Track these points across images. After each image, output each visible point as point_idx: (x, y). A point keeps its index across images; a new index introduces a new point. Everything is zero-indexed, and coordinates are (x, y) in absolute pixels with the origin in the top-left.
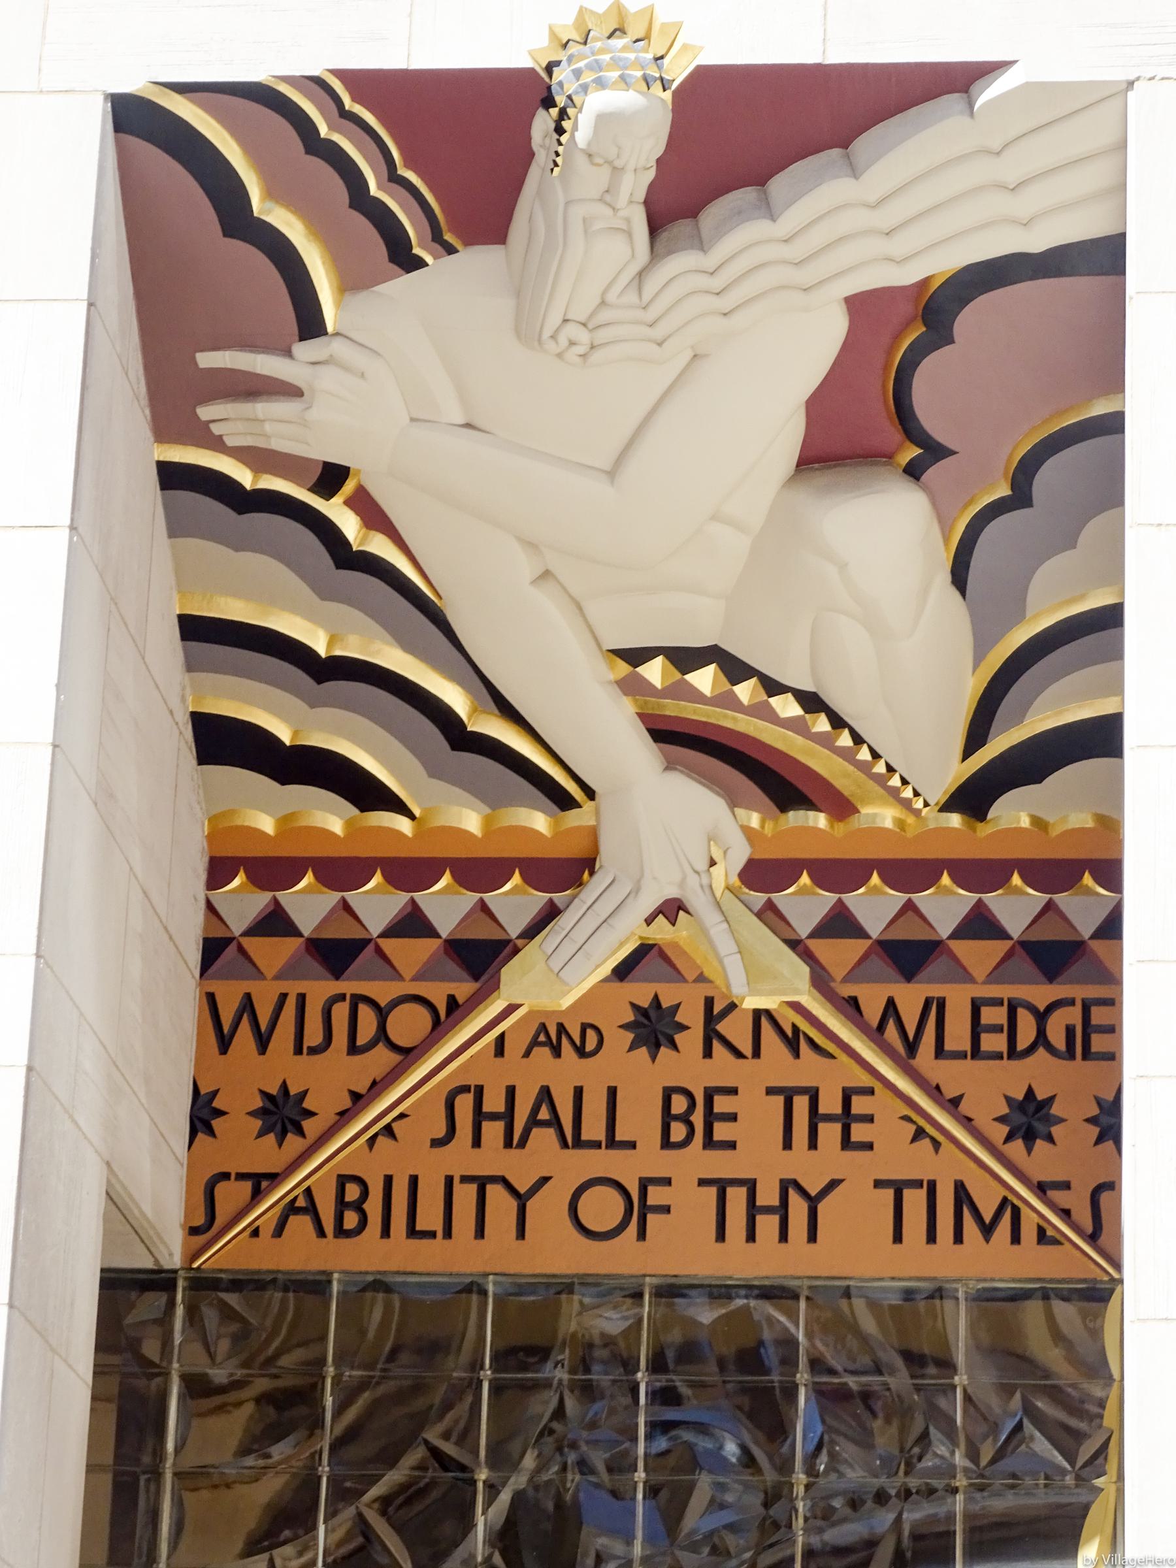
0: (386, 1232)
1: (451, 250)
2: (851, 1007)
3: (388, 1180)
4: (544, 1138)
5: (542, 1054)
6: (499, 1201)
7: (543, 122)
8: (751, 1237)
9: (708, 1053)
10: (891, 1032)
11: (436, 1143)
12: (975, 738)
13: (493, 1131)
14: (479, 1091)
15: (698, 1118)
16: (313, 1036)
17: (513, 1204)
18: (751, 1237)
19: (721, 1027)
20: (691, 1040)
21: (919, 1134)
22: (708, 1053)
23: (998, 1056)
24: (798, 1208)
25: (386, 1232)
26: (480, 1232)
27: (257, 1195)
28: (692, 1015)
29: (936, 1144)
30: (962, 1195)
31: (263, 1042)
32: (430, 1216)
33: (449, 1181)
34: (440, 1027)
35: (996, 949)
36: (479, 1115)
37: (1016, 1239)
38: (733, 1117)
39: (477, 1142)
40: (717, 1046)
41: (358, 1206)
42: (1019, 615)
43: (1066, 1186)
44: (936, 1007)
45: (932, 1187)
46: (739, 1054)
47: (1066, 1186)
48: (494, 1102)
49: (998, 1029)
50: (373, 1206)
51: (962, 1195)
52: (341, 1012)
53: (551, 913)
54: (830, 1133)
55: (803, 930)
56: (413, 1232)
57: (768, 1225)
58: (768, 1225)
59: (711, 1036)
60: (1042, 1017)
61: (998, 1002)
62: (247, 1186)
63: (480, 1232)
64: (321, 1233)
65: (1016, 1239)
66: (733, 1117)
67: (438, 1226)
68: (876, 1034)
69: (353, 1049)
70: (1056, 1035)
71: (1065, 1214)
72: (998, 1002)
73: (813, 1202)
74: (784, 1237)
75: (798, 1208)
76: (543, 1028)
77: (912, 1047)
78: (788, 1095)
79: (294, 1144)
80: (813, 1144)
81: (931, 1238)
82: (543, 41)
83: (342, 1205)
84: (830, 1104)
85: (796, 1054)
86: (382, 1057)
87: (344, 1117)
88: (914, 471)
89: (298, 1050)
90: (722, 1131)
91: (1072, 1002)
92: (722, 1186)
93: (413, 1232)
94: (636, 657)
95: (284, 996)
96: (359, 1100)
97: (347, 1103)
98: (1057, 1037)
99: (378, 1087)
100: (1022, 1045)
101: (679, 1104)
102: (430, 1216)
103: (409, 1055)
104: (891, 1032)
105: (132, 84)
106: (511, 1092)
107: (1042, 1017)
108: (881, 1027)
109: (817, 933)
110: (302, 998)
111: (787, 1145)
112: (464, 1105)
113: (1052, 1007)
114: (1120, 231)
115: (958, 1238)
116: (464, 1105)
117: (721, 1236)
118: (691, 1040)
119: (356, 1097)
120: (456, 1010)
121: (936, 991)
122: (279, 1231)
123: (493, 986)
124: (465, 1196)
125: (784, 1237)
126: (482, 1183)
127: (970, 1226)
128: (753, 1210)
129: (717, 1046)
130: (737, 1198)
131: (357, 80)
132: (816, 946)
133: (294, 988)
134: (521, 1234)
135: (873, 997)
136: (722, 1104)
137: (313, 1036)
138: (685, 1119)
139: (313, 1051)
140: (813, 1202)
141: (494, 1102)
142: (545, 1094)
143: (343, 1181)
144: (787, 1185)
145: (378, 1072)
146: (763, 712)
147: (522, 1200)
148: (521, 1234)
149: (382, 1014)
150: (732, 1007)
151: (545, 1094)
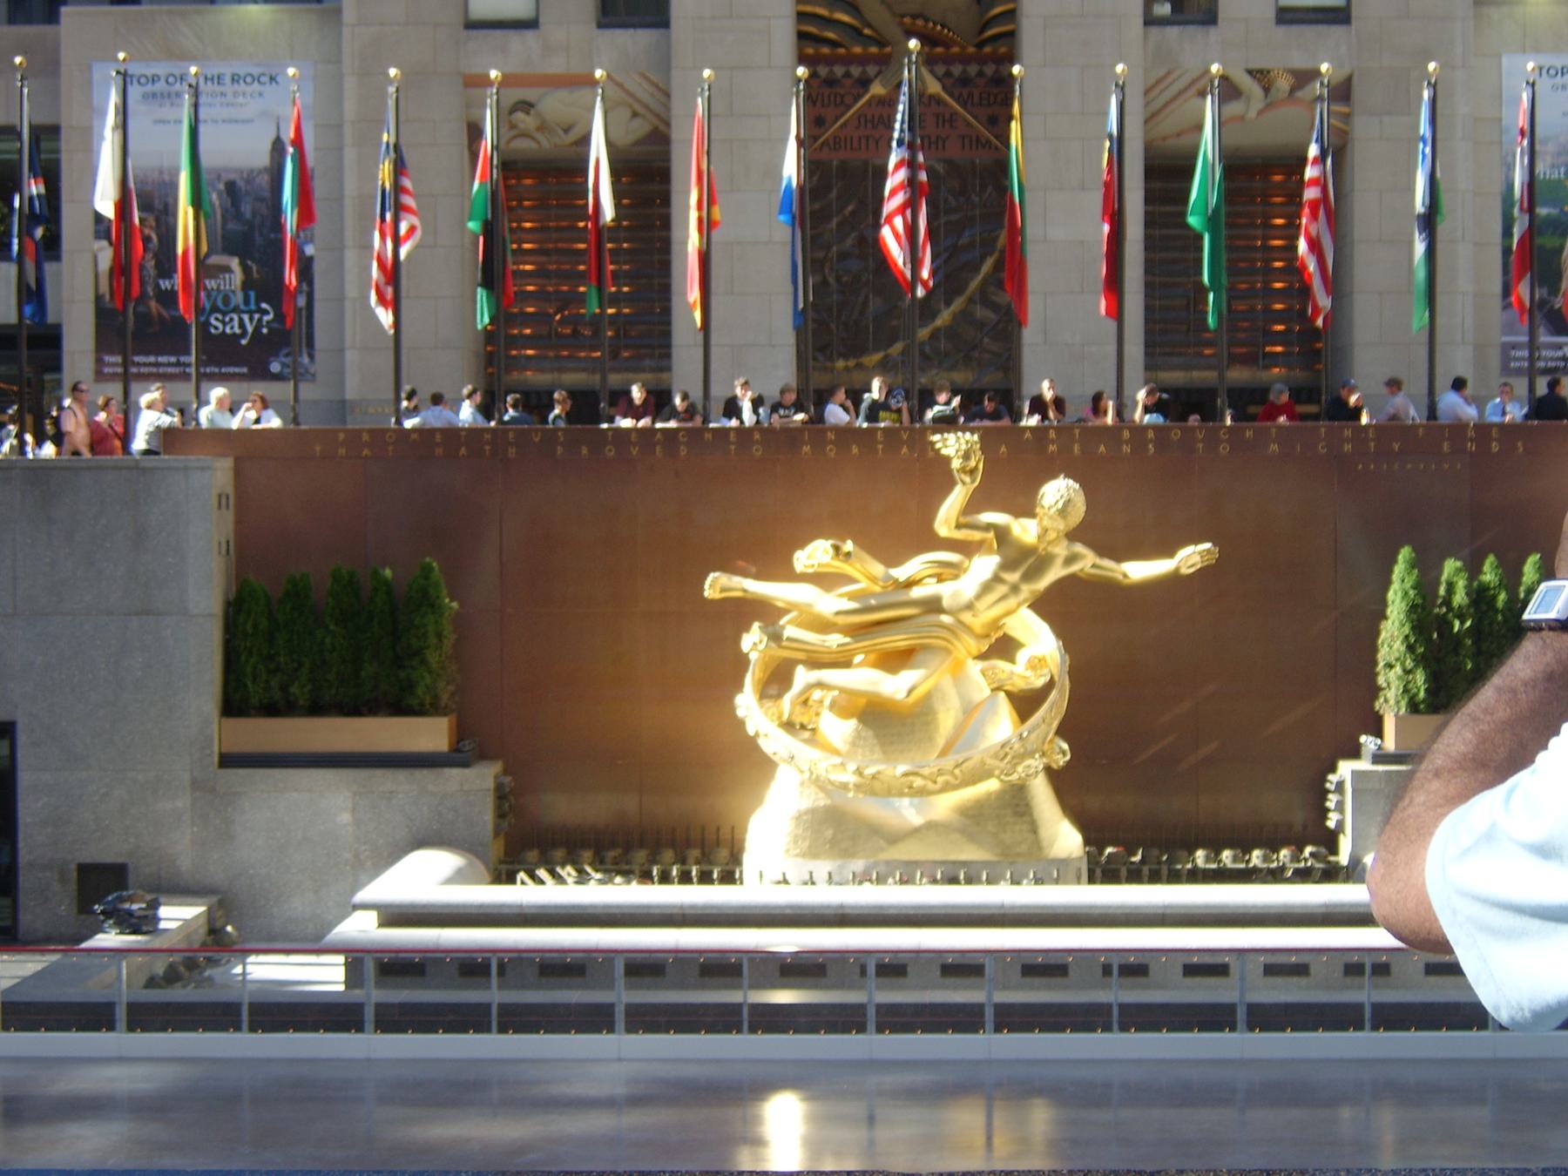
2: (951, 95)
10: (961, 100)
13: (869, 125)
16: (826, 101)
32: (855, 145)
36: (866, 121)
42: (992, 6)
44: (971, 95)
48: (869, 117)
50: (843, 144)
54: (947, 125)
57: (933, 146)
58: (933, 146)
64: (830, 149)
68: (958, 101)
70: (999, 99)
74: (937, 148)
93: (852, 149)
102: (855, 145)
103: (849, 107)
120: (857, 98)
123: (866, 90)
124: (863, 141)
135: (956, 93)
141: (869, 117)
149: (842, 97)
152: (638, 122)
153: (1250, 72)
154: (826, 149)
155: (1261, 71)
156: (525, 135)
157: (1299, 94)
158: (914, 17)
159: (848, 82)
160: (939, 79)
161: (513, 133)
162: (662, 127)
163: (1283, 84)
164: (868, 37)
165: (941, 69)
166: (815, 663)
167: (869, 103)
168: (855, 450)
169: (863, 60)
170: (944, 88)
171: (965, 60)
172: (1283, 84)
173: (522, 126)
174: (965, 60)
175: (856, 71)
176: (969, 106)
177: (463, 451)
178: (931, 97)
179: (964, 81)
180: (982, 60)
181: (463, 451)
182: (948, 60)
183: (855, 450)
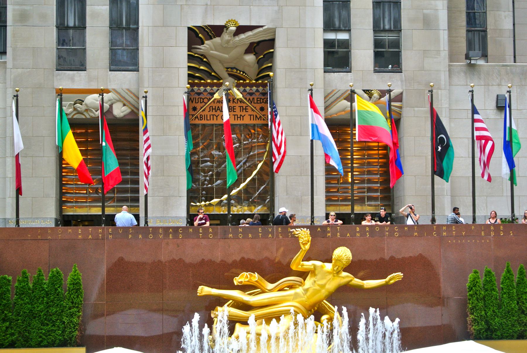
0: (205, 120)
1: (215, 38)
2: (246, 99)
3: (205, 115)
4: (218, 111)
5: (218, 103)
6: (215, 117)
7: (225, 29)
8: (237, 120)
9: (233, 103)
10: (250, 101)
11: (209, 112)
12: (258, 75)
13: (214, 110)
14: (212, 107)
15: (232, 109)
16: (197, 101)
17: (216, 117)
18: (237, 120)
19: (234, 101)
20: (231, 102)
21: (252, 110)
22: (233, 103)
23: (259, 103)
24: (242, 117)
25: (205, 120)
26: (213, 120)
27: (193, 116)
28: (231, 99)
29: (254, 111)
30: (256, 116)
31: (192, 102)
32: (209, 118)
33: (210, 115)
34: (208, 101)
35: (259, 93)
36: (213, 109)
37: (261, 120)
38: (235, 109)
39: (212, 111)
40: (234, 103)
41: (202, 117)
43: (265, 115)
44: (253, 99)
45: (253, 115)
46: (236, 103)
47: (265, 115)
48: (214, 108)
49: (259, 101)
50: (203, 117)
51: (256, 116)
52: (199, 99)
53: (218, 90)
54: (244, 110)
55: (241, 91)
56: (207, 120)
57: (239, 119)
58: (239, 119)
59: (233, 101)
60: (263, 100)
61: (259, 98)
62: (192, 116)
63: (213, 120)
64: (199, 120)
65: (261, 120)
66: (235, 109)
67: (209, 119)
68: (248, 101)
69: (201, 103)
71: (265, 118)
72: (259, 98)
73: (243, 117)
74: (240, 120)
75: (242, 117)
76: (218, 101)
77: (251, 102)
78: (240, 107)
79: (196, 112)
80: (243, 111)
81: (253, 120)
82: (226, 23)
83: (200, 117)
84: (244, 108)
85: (241, 103)
86: (203, 104)
87: (200, 109)
88: (254, 55)
89: (196, 103)
90: (235, 110)
91: (265, 98)
92: (235, 115)
93: (207, 120)
94: (227, 68)
95: (194, 98)
96: (202, 108)
97: (200, 108)
98: (264, 102)
99: (203, 106)
100: (261, 102)
101: (231, 108)
102: (209, 118)
103: (206, 103)
104: (250, 101)
105: (190, 26)
106: (215, 107)
107: (263, 100)
108: (249, 101)
109: (243, 91)
110: (196, 98)
111: (240, 111)
112: (211, 108)
113: (264, 99)
114: (274, 38)
115: (256, 120)
116: (211, 108)
117: (235, 120)
118: (231, 102)
119: (201, 107)
120: (210, 99)
121: (254, 97)
122: (195, 120)
123: (213, 97)
124: (212, 116)
125: (240, 120)
126: (213, 115)
127: (257, 119)
128: (238, 117)
129: (234, 103)
130: (236, 116)
131: (209, 26)
132: (242, 93)
133: (195, 97)
134: (217, 120)
136: (234, 108)
137: (197, 101)
138: (231, 109)
139: (197, 103)
140: (243, 117)
141: (214, 108)
142: (218, 107)
143: (200, 115)
144: (241, 115)
145: (203, 105)
146: (239, 73)
147: (217, 117)
148: (217, 120)
149: (203, 99)
150: (235, 99)
151: (218, 107)
152: (124, 108)
153: (364, 91)
154: (197, 119)
155: (368, 90)
156: (79, 113)
157: (382, 99)
158: (232, 68)
159: (205, 93)
160: (241, 93)
161: (75, 112)
162: (135, 110)
164: (213, 75)
165: (242, 88)
167: (214, 101)
168: (250, 236)
169: (212, 85)
170: (243, 96)
171: (251, 85)
172: (376, 95)
173: (79, 109)
174: (251, 85)
175: (208, 88)
176: (253, 103)
177: (90, 237)
178: (238, 99)
179: (251, 94)
180: (257, 86)
181: (90, 237)
182: (245, 85)
183: (250, 236)
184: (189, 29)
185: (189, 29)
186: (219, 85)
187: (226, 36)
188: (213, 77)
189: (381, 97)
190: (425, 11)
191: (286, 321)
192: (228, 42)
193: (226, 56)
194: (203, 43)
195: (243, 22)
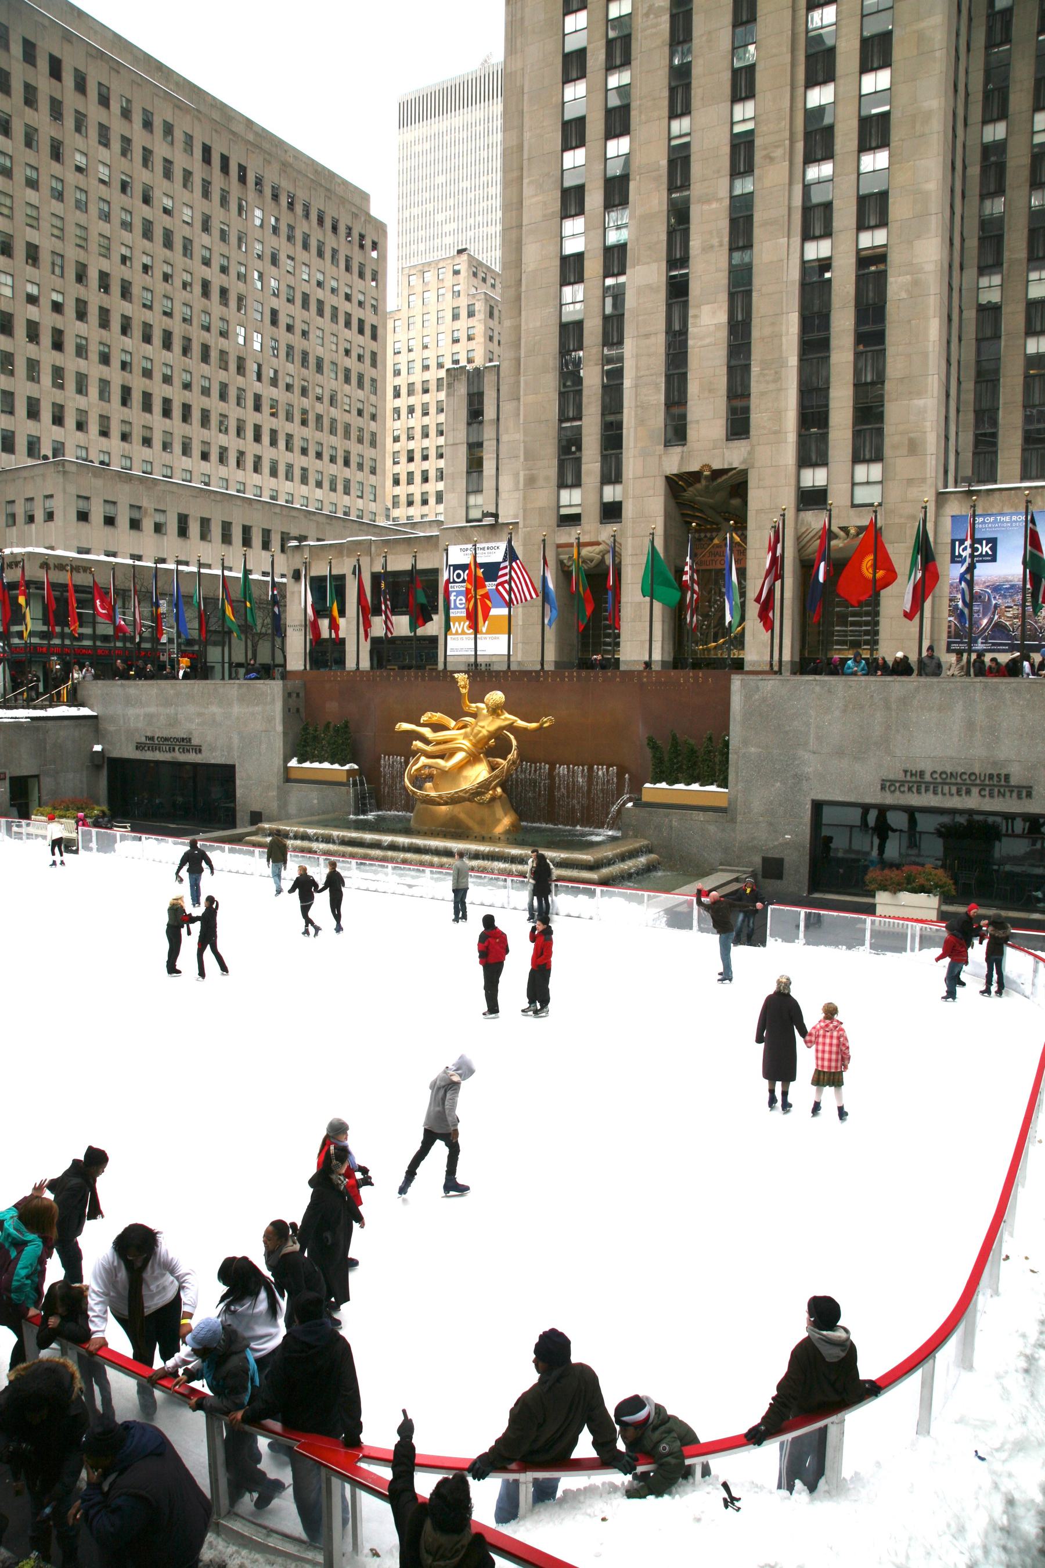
163: (853, 531)
165: (740, 533)
166: (429, 756)
169: (711, 530)
172: (853, 531)
175: (708, 535)
184: (667, 477)
185: (667, 477)
186: (718, 530)
187: (704, 482)
188: (713, 523)
189: (858, 534)
190: (912, 435)
191: (459, 756)
192: (707, 487)
193: (711, 501)
194: (685, 491)
195: (716, 466)
